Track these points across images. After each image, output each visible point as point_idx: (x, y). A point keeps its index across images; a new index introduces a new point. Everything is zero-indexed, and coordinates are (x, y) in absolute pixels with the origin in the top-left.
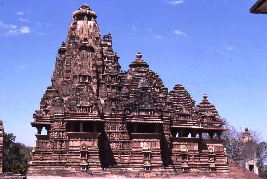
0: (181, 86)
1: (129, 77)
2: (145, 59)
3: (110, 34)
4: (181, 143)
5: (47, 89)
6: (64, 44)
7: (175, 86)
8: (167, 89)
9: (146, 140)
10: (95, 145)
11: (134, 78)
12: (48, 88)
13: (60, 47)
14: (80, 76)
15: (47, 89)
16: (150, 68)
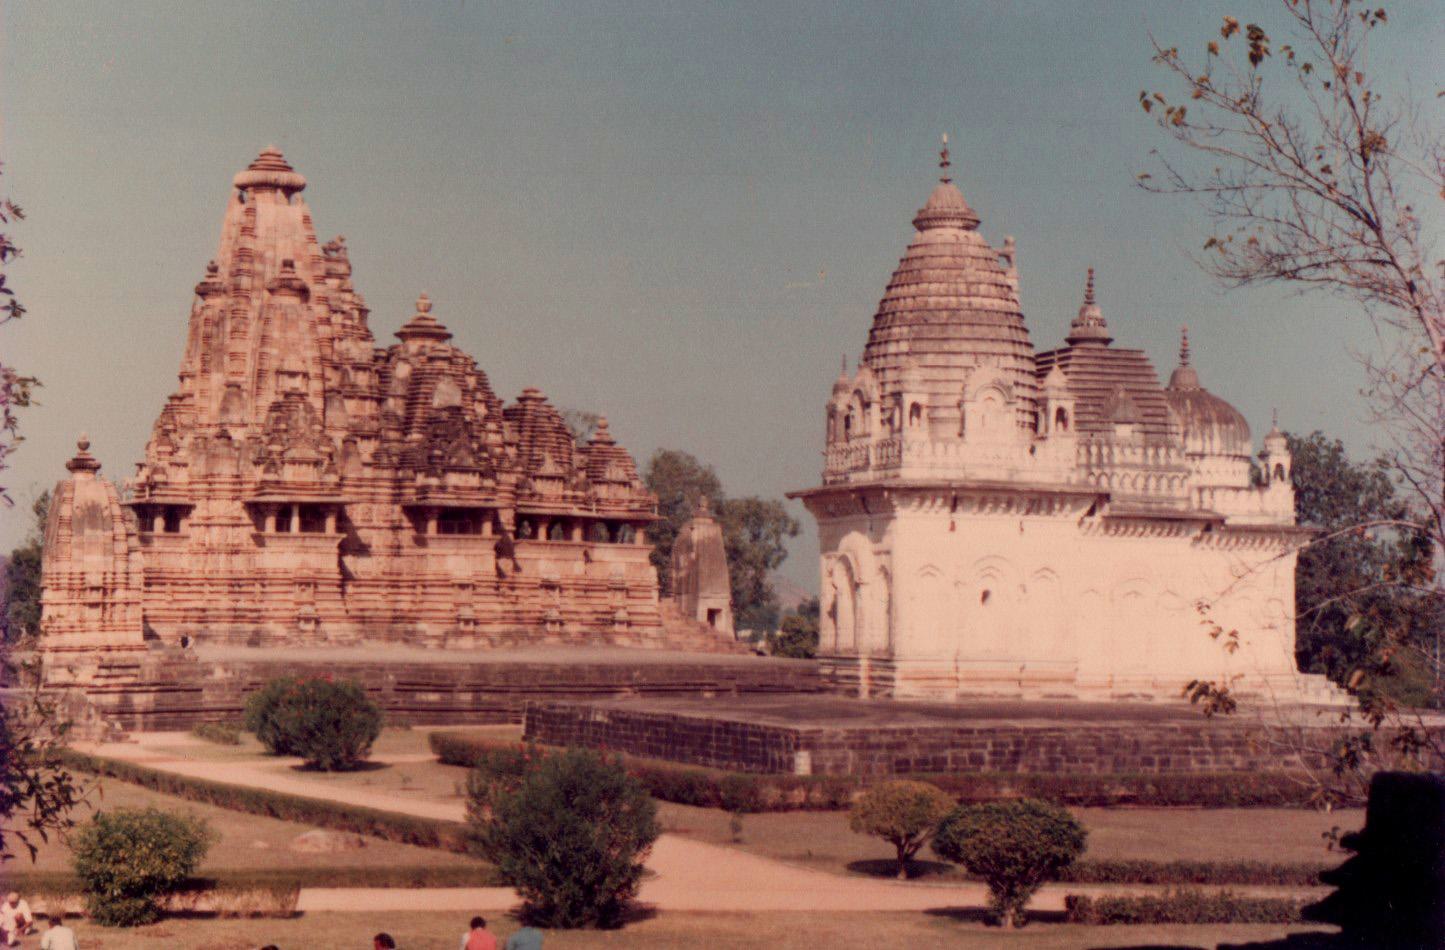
0: (539, 395)
1: (402, 371)
2: (439, 317)
3: (342, 240)
4: (542, 556)
5: (168, 402)
6: (214, 269)
7: (520, 394)
8: (501, 402)
9: (463, 552)
10: (330, 565)
11: (417, 379)
12: (172, 398)
13: (201, 276)
14: (279, 372)
15: (168, 402)
16: (455, 342)
